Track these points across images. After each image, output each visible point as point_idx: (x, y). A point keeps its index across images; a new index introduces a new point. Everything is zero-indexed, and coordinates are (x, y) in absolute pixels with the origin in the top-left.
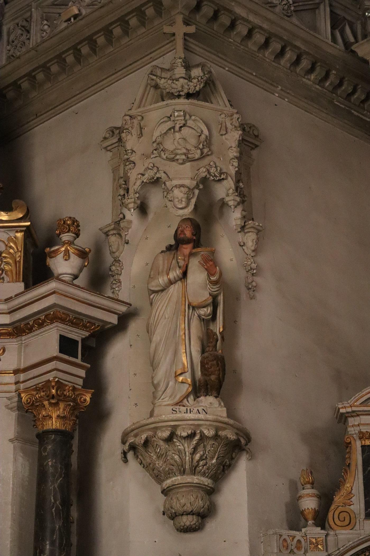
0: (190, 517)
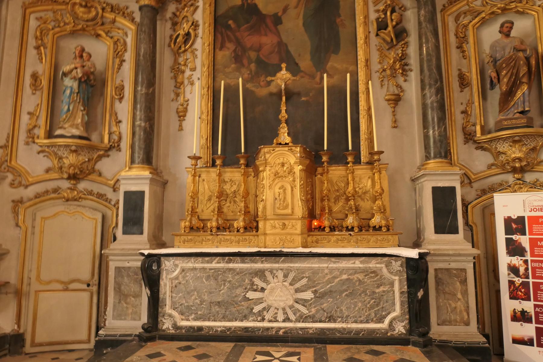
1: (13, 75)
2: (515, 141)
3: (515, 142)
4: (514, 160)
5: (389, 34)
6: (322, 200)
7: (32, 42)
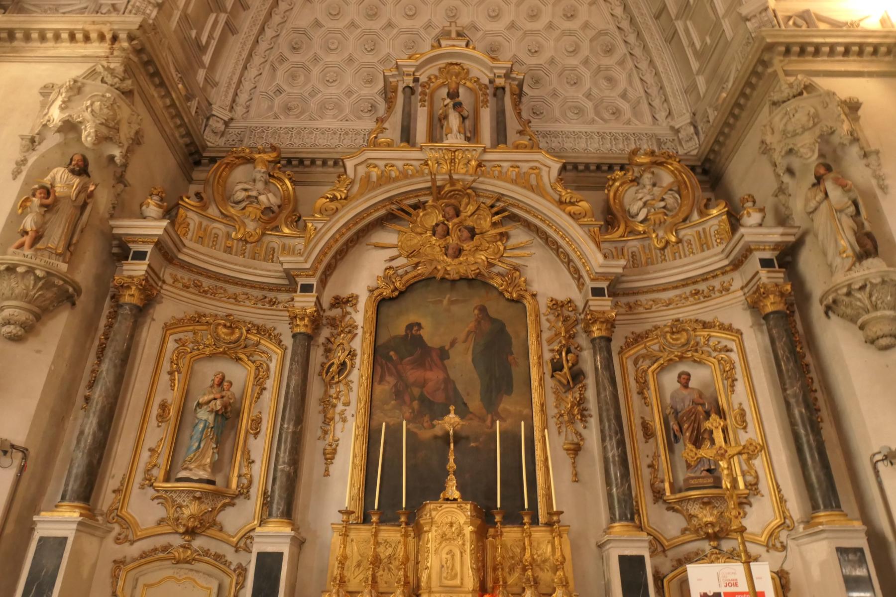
0: (884, 339)
1: (142, 404)
2: (706, 503)
3: (705, 504)
4: (706, 525)
5: (565, 375)
6: (495, 569)
7: (166, 366)
